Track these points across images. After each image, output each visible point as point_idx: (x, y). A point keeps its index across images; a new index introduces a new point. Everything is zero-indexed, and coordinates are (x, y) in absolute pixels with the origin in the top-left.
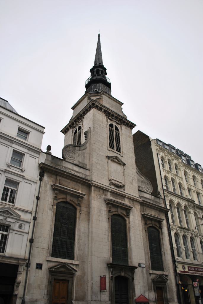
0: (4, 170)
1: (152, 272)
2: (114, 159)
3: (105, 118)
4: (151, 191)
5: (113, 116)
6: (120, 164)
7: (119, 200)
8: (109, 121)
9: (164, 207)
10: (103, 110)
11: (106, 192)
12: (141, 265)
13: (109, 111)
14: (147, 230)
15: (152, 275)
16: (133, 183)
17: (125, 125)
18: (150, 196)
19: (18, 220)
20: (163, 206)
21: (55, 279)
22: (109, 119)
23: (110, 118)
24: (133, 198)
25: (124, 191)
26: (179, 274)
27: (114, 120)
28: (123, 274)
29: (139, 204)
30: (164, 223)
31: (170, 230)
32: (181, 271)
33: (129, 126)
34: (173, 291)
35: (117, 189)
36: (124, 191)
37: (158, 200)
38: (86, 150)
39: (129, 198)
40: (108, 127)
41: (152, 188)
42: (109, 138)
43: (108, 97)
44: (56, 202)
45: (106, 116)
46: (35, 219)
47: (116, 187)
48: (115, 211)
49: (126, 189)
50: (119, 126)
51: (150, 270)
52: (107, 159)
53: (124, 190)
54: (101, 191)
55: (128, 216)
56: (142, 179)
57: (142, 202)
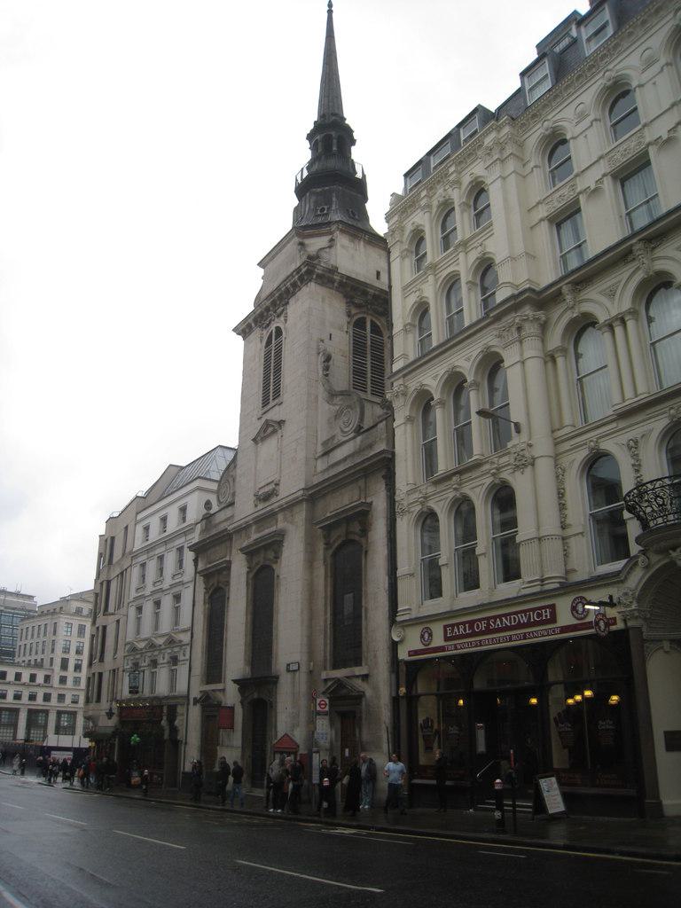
5: (267, 309)
6: (274, 432)
7: (267, 531)
8: (265, 332)
10: (253, 325)
14: (329, 561)
19: (181, 646)
21: (208, 716)
26: (407, 663)
28: (256, 696)
32: (411, 653)
34: (380, 719)
35: (267, 504)
36: (279, 498)
39: (282, 509)
43: (271, 260)
46: (192, 637)
48: (257, 564)
50: (282, 318)
51: (325, 669)
55: (277, 557)
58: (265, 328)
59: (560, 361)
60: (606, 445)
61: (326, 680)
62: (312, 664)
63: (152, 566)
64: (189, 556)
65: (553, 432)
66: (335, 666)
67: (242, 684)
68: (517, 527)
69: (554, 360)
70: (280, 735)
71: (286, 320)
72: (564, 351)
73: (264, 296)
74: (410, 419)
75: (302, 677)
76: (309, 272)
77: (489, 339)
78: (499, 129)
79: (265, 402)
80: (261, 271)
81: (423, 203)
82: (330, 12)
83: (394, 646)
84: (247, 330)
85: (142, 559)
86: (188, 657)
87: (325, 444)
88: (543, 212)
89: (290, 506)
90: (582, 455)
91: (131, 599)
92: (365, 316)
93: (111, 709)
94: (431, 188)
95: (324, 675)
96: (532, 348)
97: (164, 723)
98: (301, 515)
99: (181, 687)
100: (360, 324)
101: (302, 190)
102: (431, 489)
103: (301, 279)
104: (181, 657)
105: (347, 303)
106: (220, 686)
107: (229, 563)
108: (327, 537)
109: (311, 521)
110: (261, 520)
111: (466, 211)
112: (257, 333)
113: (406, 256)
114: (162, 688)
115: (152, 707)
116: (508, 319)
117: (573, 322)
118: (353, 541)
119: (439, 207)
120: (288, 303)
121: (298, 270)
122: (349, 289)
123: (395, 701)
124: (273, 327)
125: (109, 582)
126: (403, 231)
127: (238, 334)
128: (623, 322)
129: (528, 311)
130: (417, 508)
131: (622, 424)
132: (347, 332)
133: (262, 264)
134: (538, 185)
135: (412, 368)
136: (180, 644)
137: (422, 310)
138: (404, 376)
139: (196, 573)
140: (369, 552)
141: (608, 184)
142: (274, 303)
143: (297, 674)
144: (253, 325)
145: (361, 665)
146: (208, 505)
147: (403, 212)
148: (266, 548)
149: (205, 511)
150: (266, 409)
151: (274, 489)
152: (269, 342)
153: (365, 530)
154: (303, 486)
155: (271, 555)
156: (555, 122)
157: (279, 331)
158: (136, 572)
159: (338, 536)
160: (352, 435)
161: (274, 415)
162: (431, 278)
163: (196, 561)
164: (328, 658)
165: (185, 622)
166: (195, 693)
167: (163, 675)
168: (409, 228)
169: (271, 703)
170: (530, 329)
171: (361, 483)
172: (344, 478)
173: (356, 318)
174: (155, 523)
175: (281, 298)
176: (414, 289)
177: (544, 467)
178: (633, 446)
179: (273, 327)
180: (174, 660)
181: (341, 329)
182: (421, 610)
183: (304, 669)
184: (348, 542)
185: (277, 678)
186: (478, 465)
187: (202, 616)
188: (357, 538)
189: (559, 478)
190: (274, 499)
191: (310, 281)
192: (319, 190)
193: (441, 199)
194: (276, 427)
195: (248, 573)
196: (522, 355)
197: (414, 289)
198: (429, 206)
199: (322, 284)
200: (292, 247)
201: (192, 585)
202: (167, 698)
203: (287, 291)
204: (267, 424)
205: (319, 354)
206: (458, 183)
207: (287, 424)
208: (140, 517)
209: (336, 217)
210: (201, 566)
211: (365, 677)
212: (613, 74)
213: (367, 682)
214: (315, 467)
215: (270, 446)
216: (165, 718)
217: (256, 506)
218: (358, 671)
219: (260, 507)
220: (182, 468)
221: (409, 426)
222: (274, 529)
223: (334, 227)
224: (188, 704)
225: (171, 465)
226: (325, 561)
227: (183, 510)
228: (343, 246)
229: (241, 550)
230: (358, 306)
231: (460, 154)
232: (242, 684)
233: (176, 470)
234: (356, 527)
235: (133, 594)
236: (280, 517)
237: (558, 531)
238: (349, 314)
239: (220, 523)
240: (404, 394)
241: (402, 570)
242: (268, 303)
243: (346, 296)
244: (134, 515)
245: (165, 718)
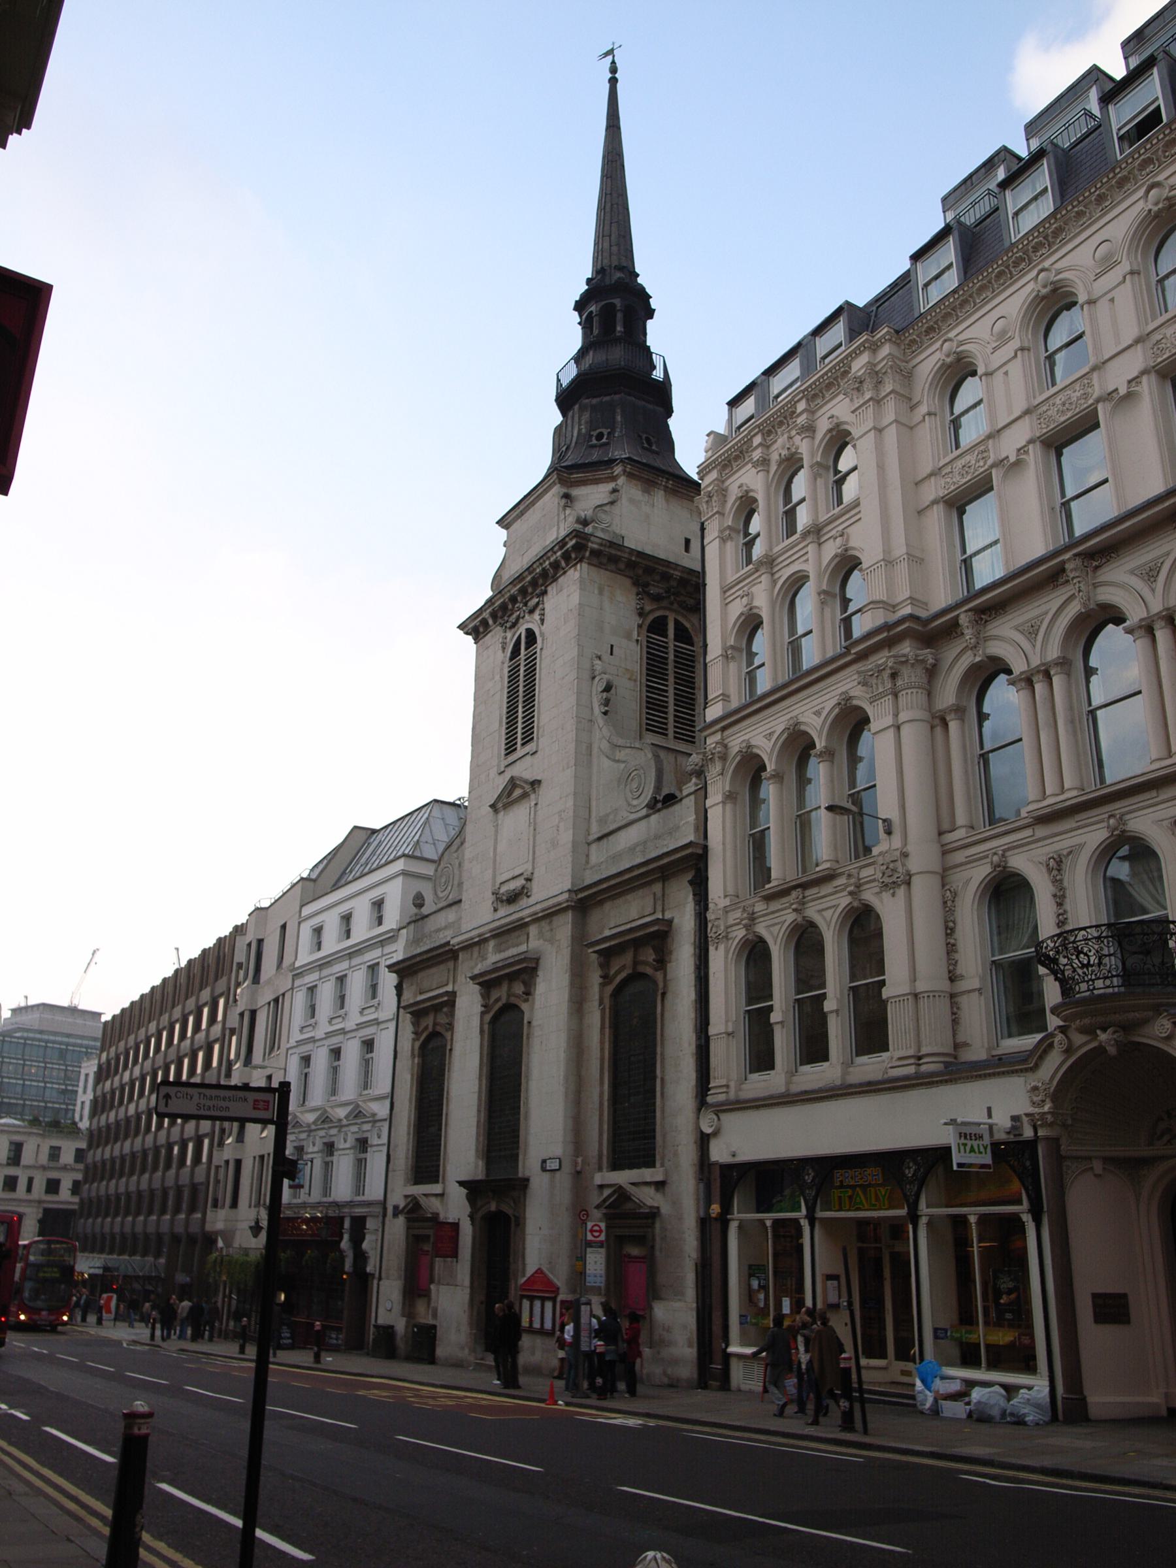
0: (355, 1027)
2: (510, 794)
5: (513, 599)
6: (525, 795)
8: (509, 635)
10: (490, 622)
14: (607, 1002)
17: (555, 579)
19: (375, 1121)
28: (493, 1207)
33: (563, 564)
36: (532, 901)
39: (537, 919)
44: (417, 1044)
50: (536, 616)
51: (600, 1169)
55: (528, 993)
56: (623, 766)
58: (511, 628)
59: (953, 726)
60: (1020, 863)
61: (601, 1187)
62: (580, 1160)
63: (327, 992)
64: (388, 981)
65: (940, 834)
66: (615, 1166)
67: (473, 1188)
68: (883, 974)
69: (945, 724)
70: (530, 1271)
71: (542, 621)
72: (959, 711)
73: (507, 576)
74: (730, 797)
75: (564, 1180)
76: (578, 548)
77: (847, 684)
78: (874, 348)
79: (510, 748)
80: (503, 534)
81: (757, 455)
82: (613, 81)
83: (704, 1141)
84: (481, 630)
85: (310, 979)
86: (384, 1140)
87: (602, 821)
88: (934, 490)
89: (549, 915)
90: (980, 873)
91: (292, 1042)
92: (667, 613)
93: (257, 1222)
94: (769, 433)
95: (599, 1179)
96: (911, 707)
97: (345, 1244)
98: (564, 927)
99: (374, 1190)
100: (657, 627)
101: (566, 399)
102: (760, 907)
103: (566, 557)
104: (374, 1140)
105: (638, 594)
106: (436, 1188)
107: (453, 995)
108: (605, 966)
109: (580, 941)
110: (503, 934)
111: (820, 476)
112: (496, 636)
113: (730, 537)
114: (342, 1190)
115: (327, 1220)
116: (881, 658)
117: (974, 669)
118: (644, 976)
119: (780, 463)
120: (545, 593)
121: (562, 543)
122: (640, 572)
123: (704, 1223)
124: (522, 630)
125: (253, 1013)
126: (725, 496)
127: (467, 633)
128: (1048, 676)
129: (906, 648)
130: (740, 933)
131: (1041, 831)
132: (637, 641)
133: (504, 522)
134: (929, 437)
135: (733, 719)
136: (375, 1120)
137: (751, 624)
138: (724, 729)
139: (398, 1008)
140: (669, 996)
141: (1034, 455)
142: (523, 591)
143: (558, 1174)
144: (490, 622)
145: (654, 1166)
146: (419, 901)
147: (725, 467)
148: (512, 977)
149: (414, 910)
150: (512, 758)
151: (523, 887)
152: (516, 652)
153: (662, 962)
154: (568, 886)
155: (519, 989)
156: (961, 343)
157: (531, 637)
158: (300, 999)
159: (622, 965)
160: (644, 812)
161: (525, 770)
162: (765, 578)
163: (399, 988)
164: (605, 1152)
165: (382, 1084)
166: (397, 1199)
167: (344, 1165)
168: (734, 493)
169: (517, 1218)
170: (909, 676)
171: (657, 888)
172: (630, 879)
173: (651, 618)
174: (331, 922)
175: (534, 583)
176: (740, 592)
177: (924, 890)
178: (1057, 866)
179: (522, 630)
180: (363, 1144)
181: (628, 636)
182: (744, 1086)
183: (567, 1168)
184: (636, 977)
185: (527, 1180)
186: (829, 877)
187: (409, 1077)
188: (649, 971)
189: (948, 906)
190: (524, 902)
191: (581, 561)
192: (595, 401)
193: (784, 452)
194: (528, 788)
195: (483, 1014)
196: (896, 715)
197: (740, 592)
198: (764, 462)
199: (600, 566)
200: (552, 499)
201: (392, 1025)
202: (351, 1204)
203: (544, 574)
204: (513, 783)
205: (594, 678)
206: (810, 429)
207: (544, 785)
208: (307, 911)
209: (618, 454)
210: (409, 997)
211: (660, 1185)
212: (1052, 277)
213: (664, 1193)
214: (588, 856)
215: (517, 818)
216: (346, 1237)
217: (495, 910)
218: (647, 1174)
219: (502, 912)
220: (374, 832)
221: (729, 807)
222: (523, 948)
223: (618, 470)
224: (385, 1215)
225: (356, 828)
226: (601, 1002)
227: (378, 905)
228: (631, 501)
229: (472, 978)
230: (656, 598)
231: (814, 383)
232: (473, 1188)
233: (364, 835)
234: (649, 955)
235: (296, 1036)
236: (533, 930)
237: (945, 985)
238: (641, 613)
239: (439, 930)
240: (724, 758)
241: (717, 1026)
242: (514, 590)
243: (636, 583)
244: (298, 908)
245: (346, 1237)
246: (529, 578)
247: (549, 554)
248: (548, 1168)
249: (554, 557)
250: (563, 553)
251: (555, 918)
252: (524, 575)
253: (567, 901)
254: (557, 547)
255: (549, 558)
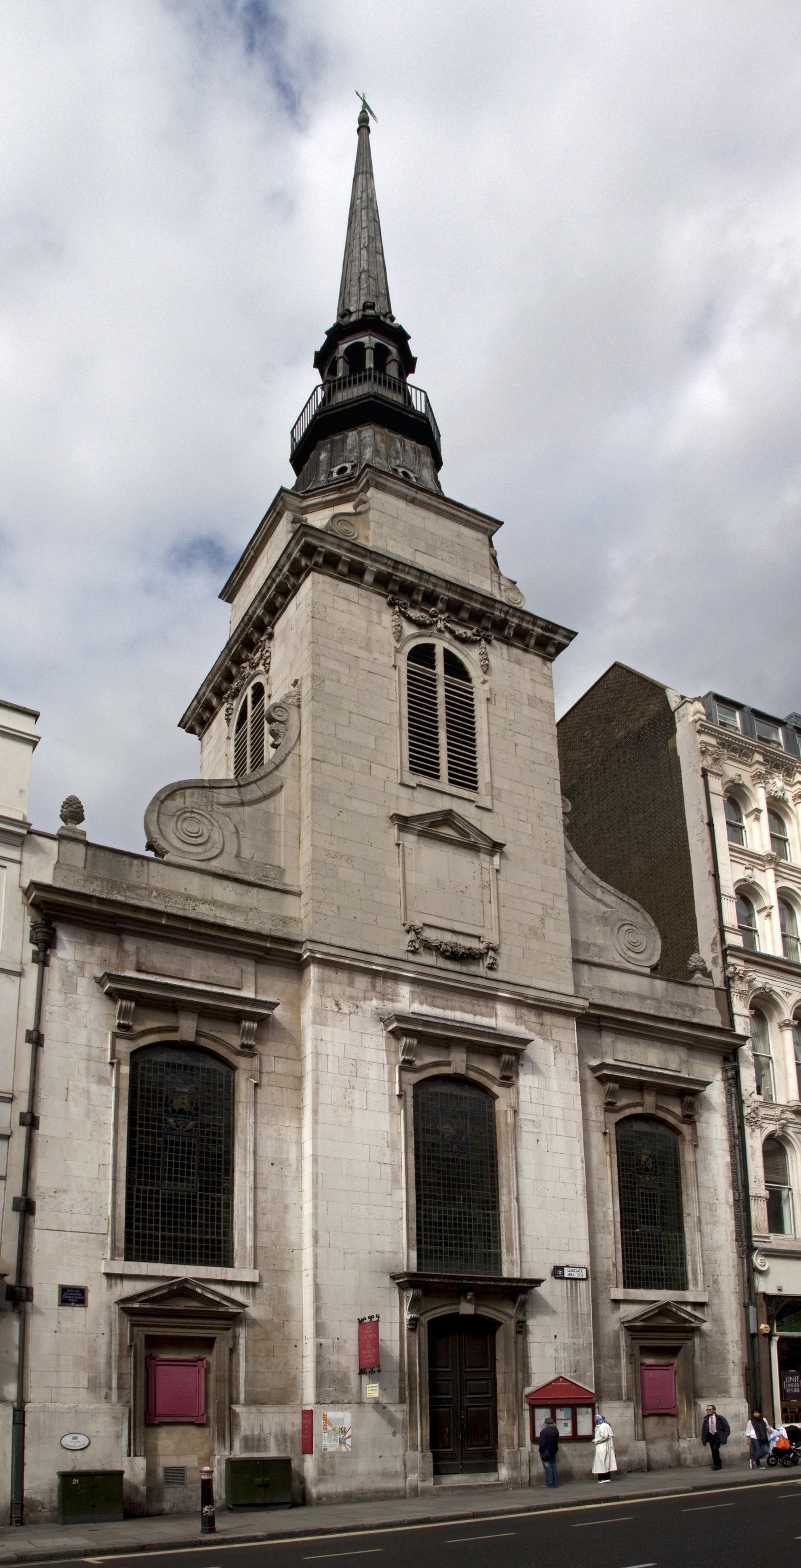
1: (625, 1294)
3: (388, 618)
4: (650, 959)
5: (430, 598)
9: (718, 1024)
11: (390, 984)
12: (567, 1273)
13: (409, 578)
15: (623, 1307)
16: (545, 931)
18: (645, 981)
20: (715, 1019)
22: (410, 620)
23: (414, 614)
24: (536, 999)
25: (492, 974)
27: (440, 625)
29: (573, 1024)
30: (716, 1093)
31: (741, 1128)
36: (492, 974)
37: (683, 994)
38: (282, 796)
40: (403, 663)
41: (659, 943)
42: (405, 722)
45: (391, 604)
47: (447, 958)
49: (502, 962)
52: (395, 830)
53: (491, 967)
54: (362, 982)
57: (588, 1015)
61: (617, 1302)
95: (618, 1293)
246: (478, 606)
247: (527, 618)
248: (566, 1275)
249: (530, 627)
250: (543, 635)
251: (548, 1019)
252: (475, 596)
253: (583, 1009)
254: (543, 624)
255: (522, 619)
